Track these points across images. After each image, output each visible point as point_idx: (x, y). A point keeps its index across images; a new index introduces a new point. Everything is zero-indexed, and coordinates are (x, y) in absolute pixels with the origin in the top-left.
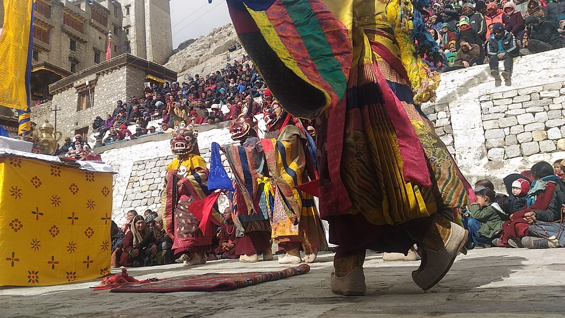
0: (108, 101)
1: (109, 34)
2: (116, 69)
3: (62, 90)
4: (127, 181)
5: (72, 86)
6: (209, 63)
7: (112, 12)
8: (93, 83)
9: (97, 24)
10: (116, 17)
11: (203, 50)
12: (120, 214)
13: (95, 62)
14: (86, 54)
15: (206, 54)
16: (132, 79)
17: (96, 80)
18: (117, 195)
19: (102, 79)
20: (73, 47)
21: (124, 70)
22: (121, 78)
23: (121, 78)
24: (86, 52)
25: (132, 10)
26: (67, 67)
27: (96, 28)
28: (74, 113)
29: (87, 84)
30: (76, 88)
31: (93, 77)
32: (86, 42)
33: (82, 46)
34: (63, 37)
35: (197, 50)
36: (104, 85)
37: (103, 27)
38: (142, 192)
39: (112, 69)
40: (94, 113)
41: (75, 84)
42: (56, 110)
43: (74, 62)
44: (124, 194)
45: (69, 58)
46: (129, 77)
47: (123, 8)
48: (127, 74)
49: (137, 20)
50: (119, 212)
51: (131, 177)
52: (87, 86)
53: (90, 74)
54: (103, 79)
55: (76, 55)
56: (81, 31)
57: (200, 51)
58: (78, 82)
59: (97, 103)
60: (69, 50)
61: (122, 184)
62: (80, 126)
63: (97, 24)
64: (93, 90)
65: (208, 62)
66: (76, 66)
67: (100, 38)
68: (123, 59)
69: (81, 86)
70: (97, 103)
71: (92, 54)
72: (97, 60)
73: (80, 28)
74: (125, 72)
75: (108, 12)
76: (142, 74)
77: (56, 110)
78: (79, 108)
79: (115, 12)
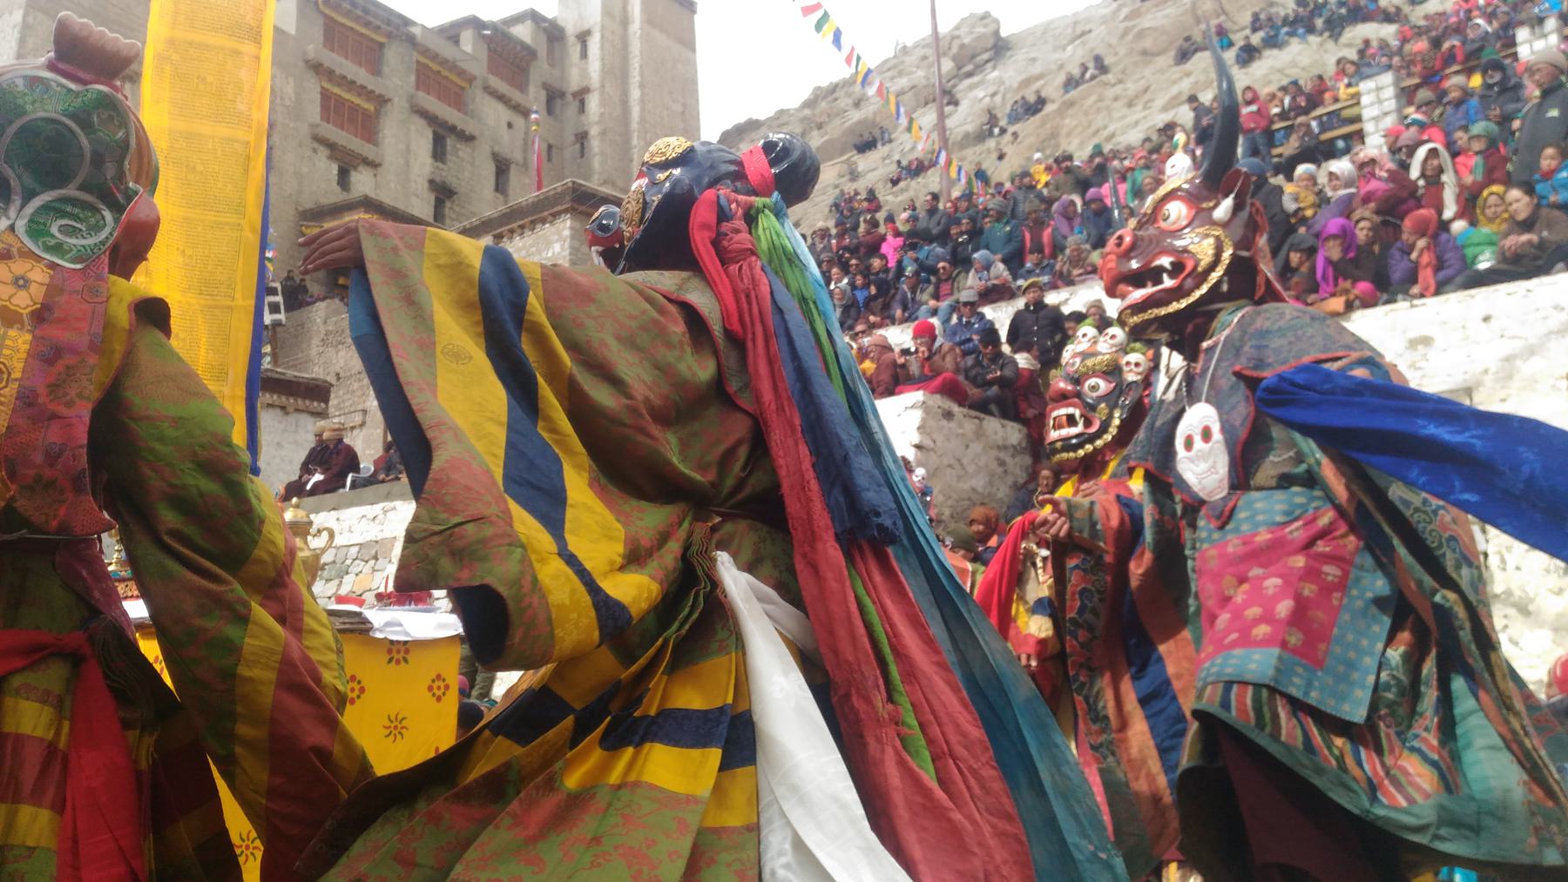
1: (533, 116)
9: (503, 87)
10: (552, 65)
13: (497, 189)
14: (472, 173)
20: (439, 153)
24: (472, 164)
26: (422, 206)
27: (501, 98)
33: (464, 150)
34: (413, 127)
37: (516, 96)
43: (443, 193)
45: (431, 182)
47: (571, 39)
49: (605, 72)
55: (449, 174)
60: (429, 160)
63: (503, 87)
66: (448, 204)
71: (489, 169)
72: (501, 186)
73: (457, 99)
75: (531, 53)
79: (550, 52)
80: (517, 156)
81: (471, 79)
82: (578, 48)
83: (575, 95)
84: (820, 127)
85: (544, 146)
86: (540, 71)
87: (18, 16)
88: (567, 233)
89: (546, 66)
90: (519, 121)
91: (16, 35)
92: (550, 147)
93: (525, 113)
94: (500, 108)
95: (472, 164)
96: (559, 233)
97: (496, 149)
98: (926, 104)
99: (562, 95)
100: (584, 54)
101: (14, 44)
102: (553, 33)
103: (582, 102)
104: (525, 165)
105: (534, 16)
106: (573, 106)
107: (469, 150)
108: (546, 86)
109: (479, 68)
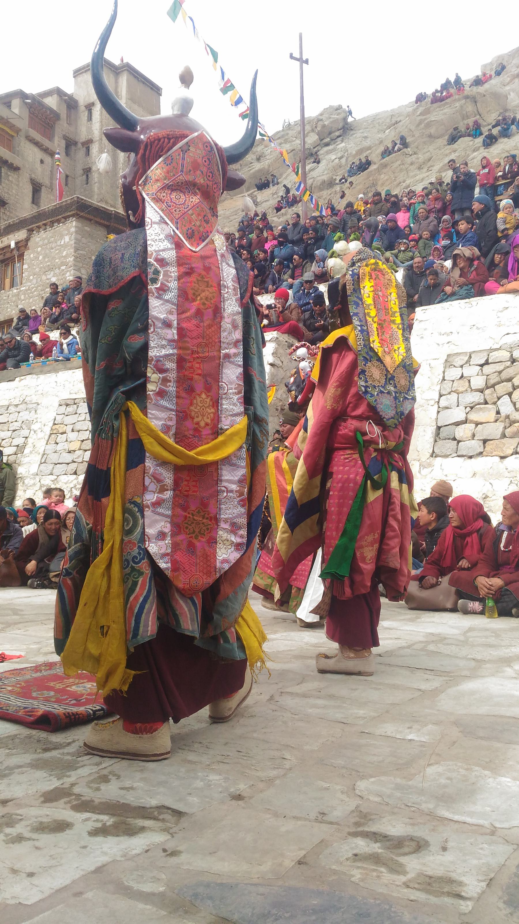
0: (44, 278)
1: (57, 156)
2: (59, 221)
4: (47, 430)
7: (63, 114)
8: (22, 246)
9: (38, 137)
10: (69, 124)
12: (34, 484)
13: (33, 202)
16: (84, 240)
17: (27, 240)
18: (31, 452)
21: (72, 225)
22: (67, 239)
23: (67, 239)
24: (18, 185)
27: (37, 144)
29: (13, 245)
31: (22, 235)
32: (17, 169)
33: (12, 176)
36: (39, 249)
37: (46, 143)
38: (70, 452)
39: (52, 223)
40: (22, 297)
44: (42, 452)
46: (79, 237)
47: (82, 108)
48: (76, 232)
50: (32, 482)
51: (55, 424)
52: (12, 250)
53: (18, 229)
54: (38, 239)
56: (10, 147)
59: (28, 280)
61: (40, 435)
63: (38, 137)
64: (21, 256)
68: (71, 204)
70: (28, 280)
71: (28, 190)
72: (35, 200)
74: (73, 229)
76: (100, 232)
79: (68, 116)
80: (46, 181)
81: (18, 131)
82: (86, 113)
83: (83, 144)
85: (64, 176)
86: (62, 127)
89: (65, 125)
90: (48, 159)
92: (67, 176)
93: (52, 154)
94: (36, 150)
95: (18, 185)
97: (33, 176)
99: (76, 143)
100: (90, 118)
102: (71, 104)
103: (88, 150)
104: (51, 188)
105: (59, 92)
106: (82, 152)
107: (16, 176)
108: (65, 138)
109: (23, 124)
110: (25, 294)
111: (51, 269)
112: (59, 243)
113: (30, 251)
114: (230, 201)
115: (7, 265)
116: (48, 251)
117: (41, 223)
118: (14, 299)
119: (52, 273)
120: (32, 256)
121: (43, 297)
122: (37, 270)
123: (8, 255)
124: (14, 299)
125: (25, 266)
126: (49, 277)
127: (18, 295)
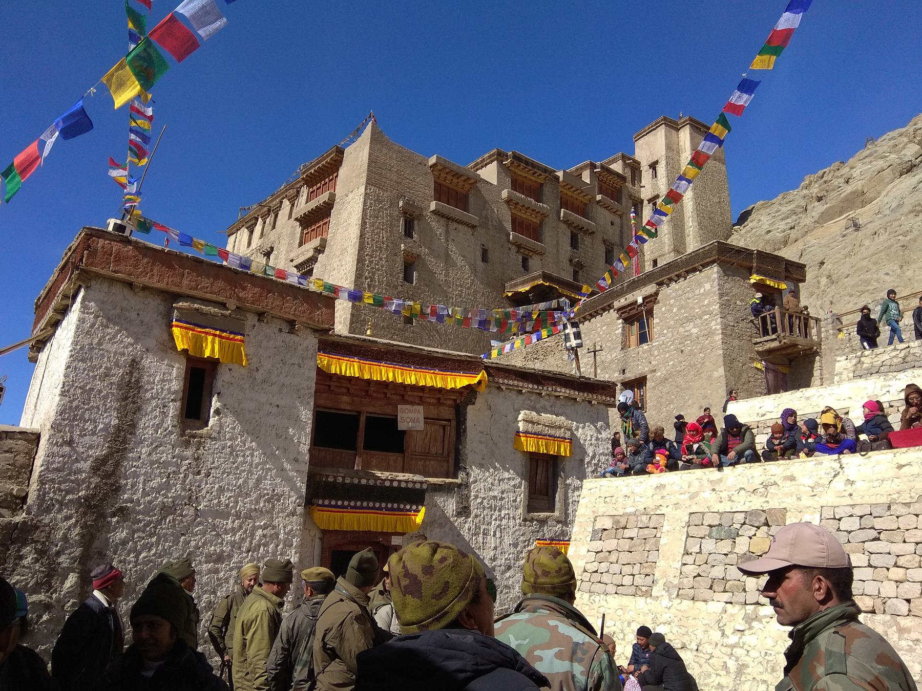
0: (681, 330)
3: (592, 316)
5: (610, 307)
6: (811, 239)
11: (794, 217)
15: (802, 224)
19: (665, 291)
25: (661, 169)
28: (617, 353)
29: (640, 300)
30: (619, 310)
31: (650, 289)
35: (782, 219)
36: (672, 301)
40: (656, 353)
41: (617, 304)
42: (595, 352)
52: (641, 305)
53: (645, 285)
57: (789, 220)
58: (622, 300)
62: (630, 376)
65: (808, 238)
67: (612, 224)
69: (629, 305)
70: (661, 334)
77: (595, 352)
78: (625, 346)
84: (820, 199)
87: (362, 189)
88: (715, 276)
91: (362, 200)
96: (709, 278)
98: (901, 175)
101: (361, 205)
110: (659, 350)
111: (689, 320)
112: (697, 292)
113: (660, 305)
114: (821, 230)
115: (632, 324)
116: (683, 302)
117: (673, 275)
118: (645, 355)
119: (692, 324)
120: (663, 309)
121: (682, 351)
122: (672, 322)
123: (632, 313)
124: (645, 355)
125: (656, 321)
126: (687, 329)
127: (650, 350)
